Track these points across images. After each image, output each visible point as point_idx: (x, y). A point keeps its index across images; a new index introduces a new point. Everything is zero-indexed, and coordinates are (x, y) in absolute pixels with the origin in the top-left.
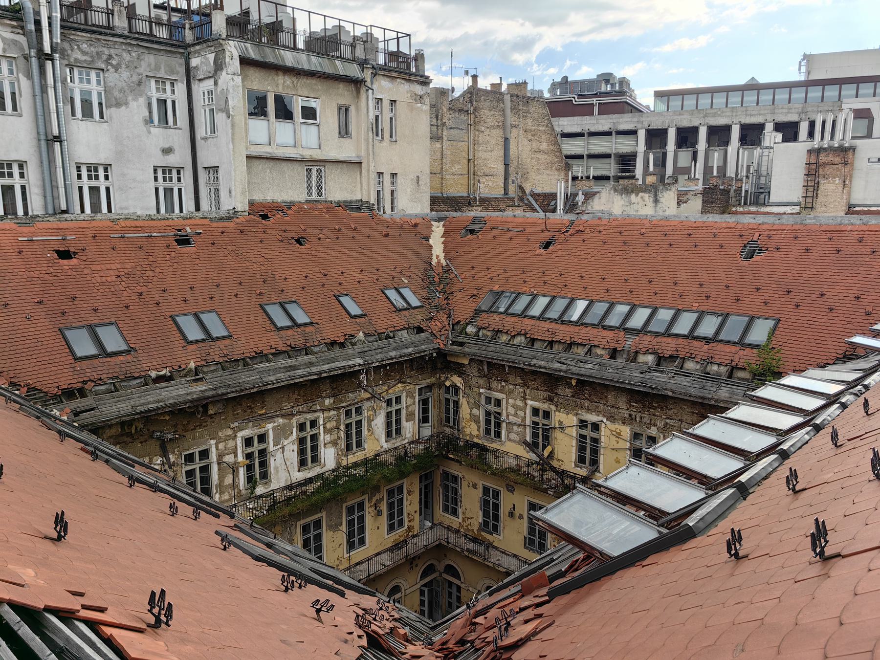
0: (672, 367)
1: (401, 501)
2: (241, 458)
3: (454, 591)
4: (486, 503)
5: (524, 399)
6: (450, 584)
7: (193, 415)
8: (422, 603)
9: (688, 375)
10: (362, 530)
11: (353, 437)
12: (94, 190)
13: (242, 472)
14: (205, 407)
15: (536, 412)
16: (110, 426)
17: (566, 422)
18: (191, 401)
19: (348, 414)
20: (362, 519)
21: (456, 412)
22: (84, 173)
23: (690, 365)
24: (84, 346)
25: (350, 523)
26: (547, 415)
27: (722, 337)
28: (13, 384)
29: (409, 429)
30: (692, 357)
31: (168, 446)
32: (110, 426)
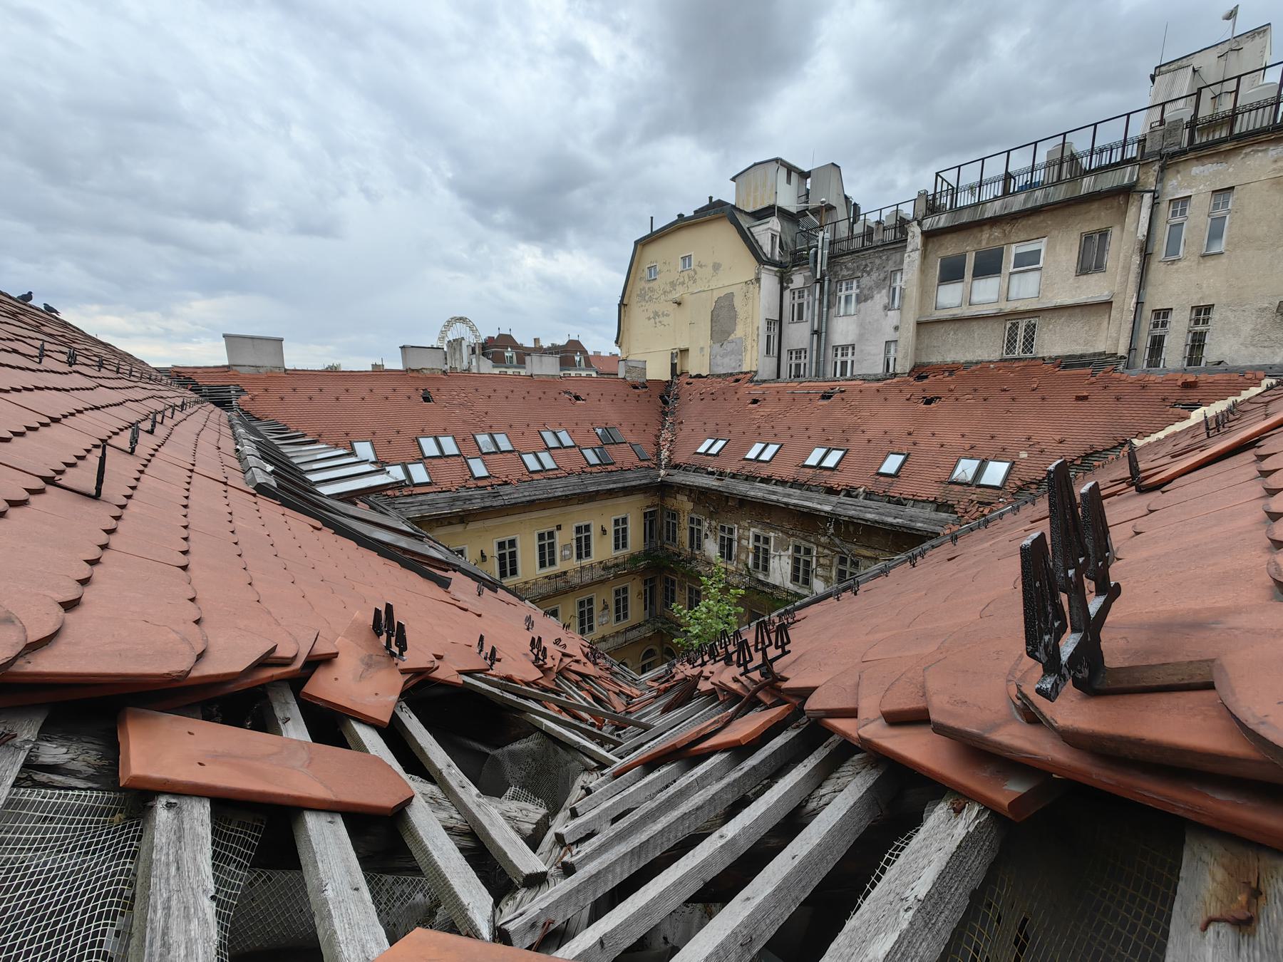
2: (751, 546)
12: (844, 364)
13: (751, 556)
19: (843, 561)
22: (839, 353)
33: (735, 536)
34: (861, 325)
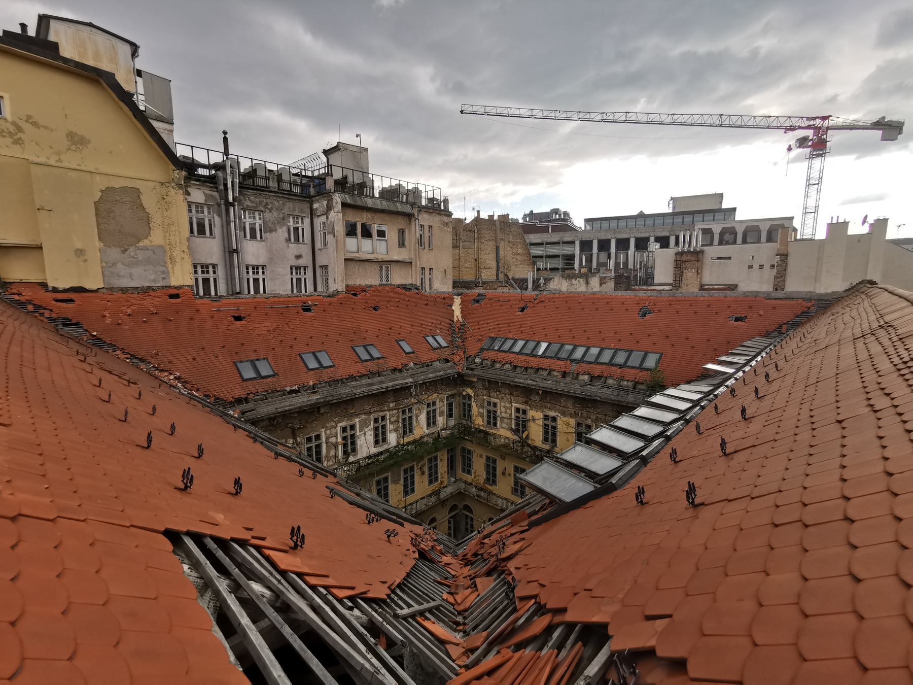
0: (599, 383)
1: (436, 465)
2: (339, 440)
3: (469, 520)
4: (488, 466)
5: (511, 402)
6: (467, 516)
7: (312, 413)
8: (450, 528)
9: (609, 387)
10: (413, 483)
11: (407, 427)
12: (256, 281)
13: (340, 448)
14: (319, 408)
15: (518, 410)
16: (263, 421)
17: (536, 415)
18: (310, 405)
19: (404, 412)
20: (412, 476)
21: (469, 411)
22: (251, 271)
23: (610, 382)
24: (249, 373)
25: (406, 479)
26: (524, 412)
27: (628, 364)
28: (206, 396)
29: (441, 421)
30: (611, 377)
31: (297, 432)
32: (263, 421)
33: (323, 439)
34: (270, 250)
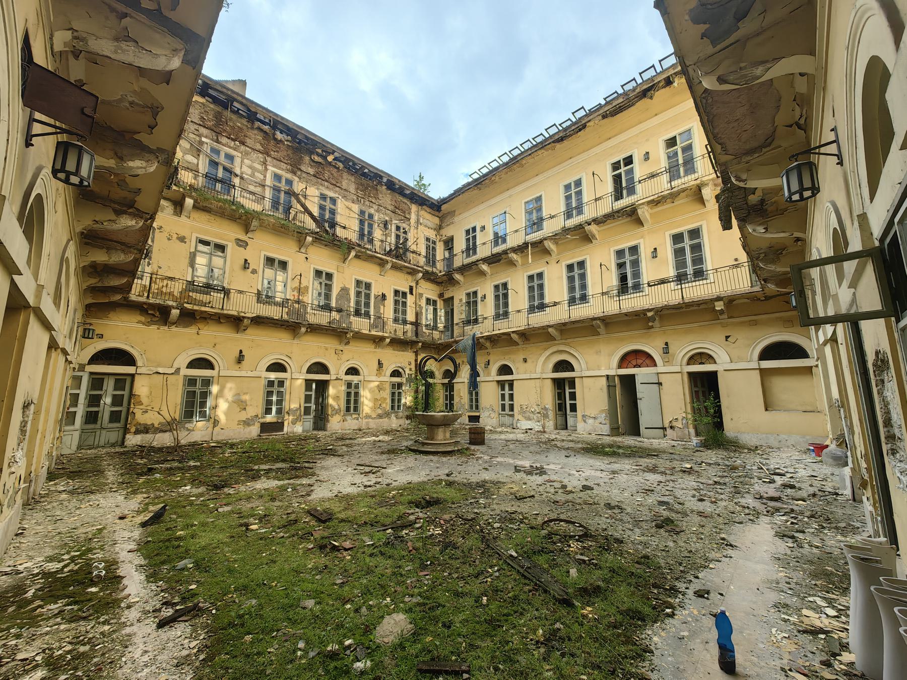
15: (277, 177)
